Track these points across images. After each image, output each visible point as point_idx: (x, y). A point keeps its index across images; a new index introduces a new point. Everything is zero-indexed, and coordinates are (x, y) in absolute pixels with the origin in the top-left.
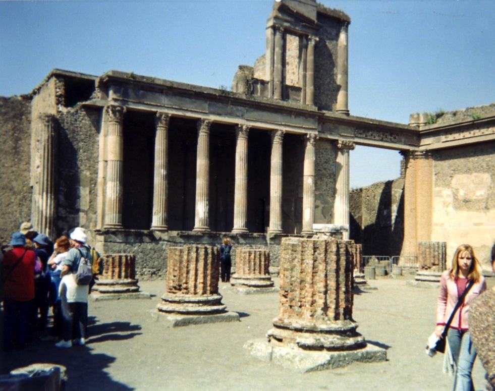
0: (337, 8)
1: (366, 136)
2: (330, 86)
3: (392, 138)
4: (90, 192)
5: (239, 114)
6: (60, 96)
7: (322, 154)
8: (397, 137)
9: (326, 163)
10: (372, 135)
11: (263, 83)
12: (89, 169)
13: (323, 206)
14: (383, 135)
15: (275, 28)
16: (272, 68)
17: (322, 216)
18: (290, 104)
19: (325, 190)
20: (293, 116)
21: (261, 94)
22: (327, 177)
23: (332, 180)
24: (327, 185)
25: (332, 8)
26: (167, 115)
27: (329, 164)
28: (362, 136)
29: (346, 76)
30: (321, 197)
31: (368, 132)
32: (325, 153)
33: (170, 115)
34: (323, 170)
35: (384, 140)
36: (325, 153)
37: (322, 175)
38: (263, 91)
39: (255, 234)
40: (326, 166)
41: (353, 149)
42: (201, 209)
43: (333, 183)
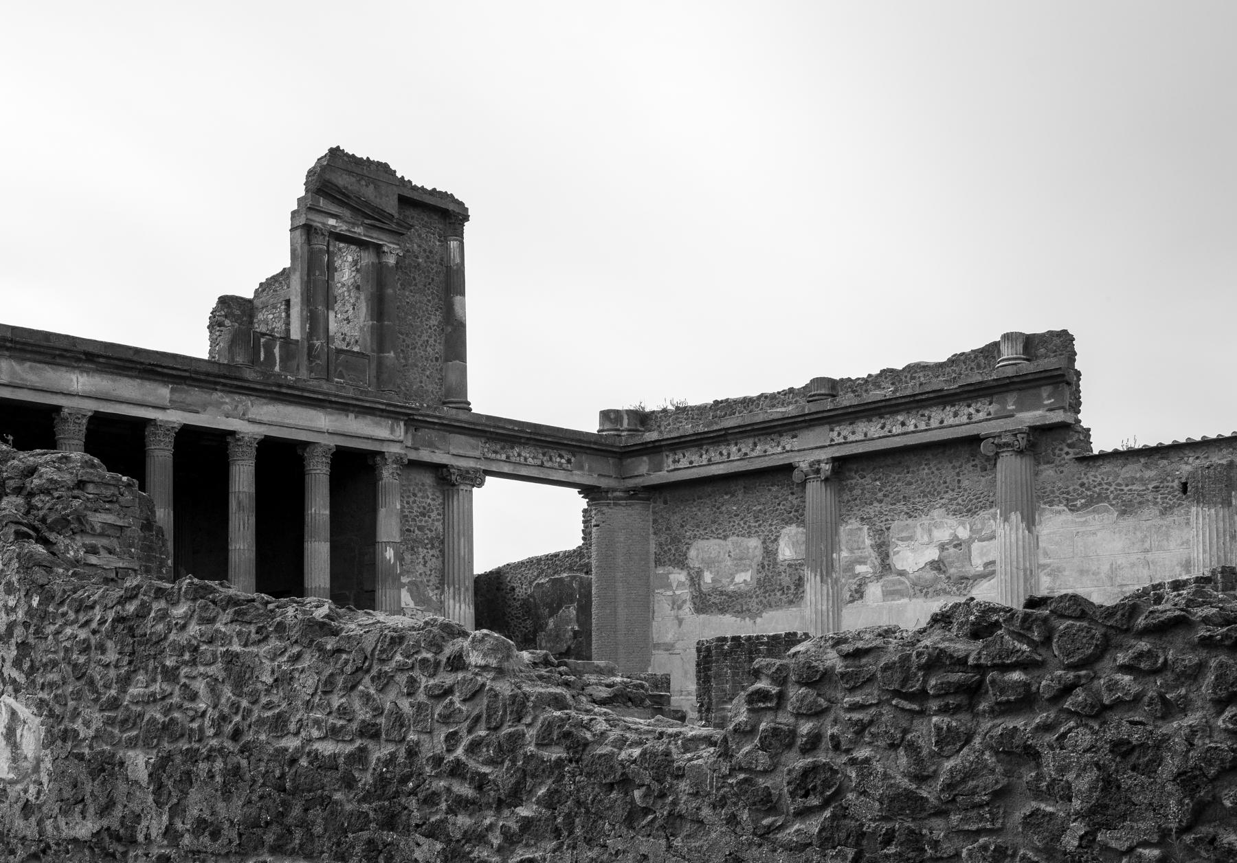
1: (508, 457)
2: (429, 349)
7: (415, 495)
9: (424, 515)
10: (519, 455)
14: (544, 455)
20: (352, 416)
22: (425, 546)
24: (425, 565)
26: (77, 414)
28: (498, 457)
31: (513, 448)
32: (420, 494)
33: (90, 414)
36: (420, 494)
37: (415, 541)
41: (480, 485)
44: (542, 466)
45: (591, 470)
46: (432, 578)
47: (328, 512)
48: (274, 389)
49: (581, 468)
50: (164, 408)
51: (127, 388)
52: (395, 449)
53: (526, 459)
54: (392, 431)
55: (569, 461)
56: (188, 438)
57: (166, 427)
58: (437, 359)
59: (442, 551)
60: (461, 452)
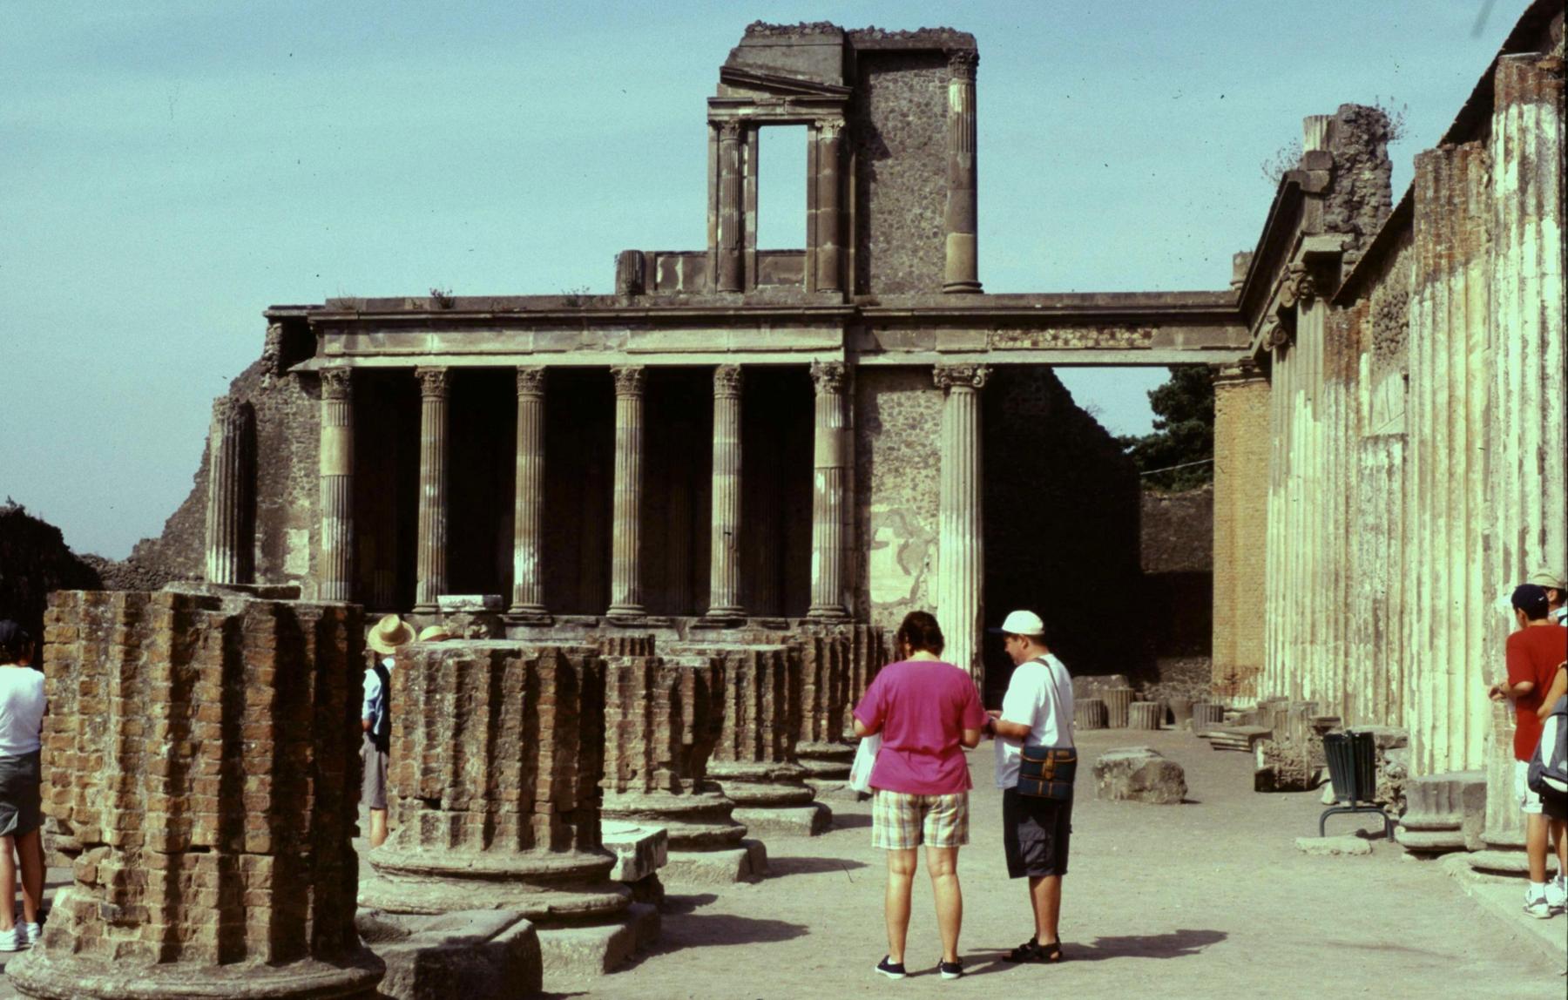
0: (933, 23)
1: (1035, 343)
2: (923, 224)
3: (1135, 336)
4: (311, 538)
5: (613, 342)
6: (270, 358)
7: (900, 404)
8: (1154, 332)
9: (913, 427)
10: (1055, 338)
12: (309, 495)
13: (902, 541)
15: (716, 125)
16: (713, 219)
17: (899, 568)
18: (767, 293)
21: (684, 282)
23: (931, 472)
24: (914, 489)
25: (913, 28)
28: (1018, 344)
29: (963, 195)
30: (897, 519)
34: (903, 447)
38: (689, 278)
39: (650, 620)
40: (913, 436)
42: (523, 565)
43: (933, 478)
44: (1096, 348)
45: (1187, 342)
46: (925, 504)
47: (733, 440)
49: (1169, 342)
56: (554, 378)
58: (935, 234)
59: (938, 470)
60: (955, 347)
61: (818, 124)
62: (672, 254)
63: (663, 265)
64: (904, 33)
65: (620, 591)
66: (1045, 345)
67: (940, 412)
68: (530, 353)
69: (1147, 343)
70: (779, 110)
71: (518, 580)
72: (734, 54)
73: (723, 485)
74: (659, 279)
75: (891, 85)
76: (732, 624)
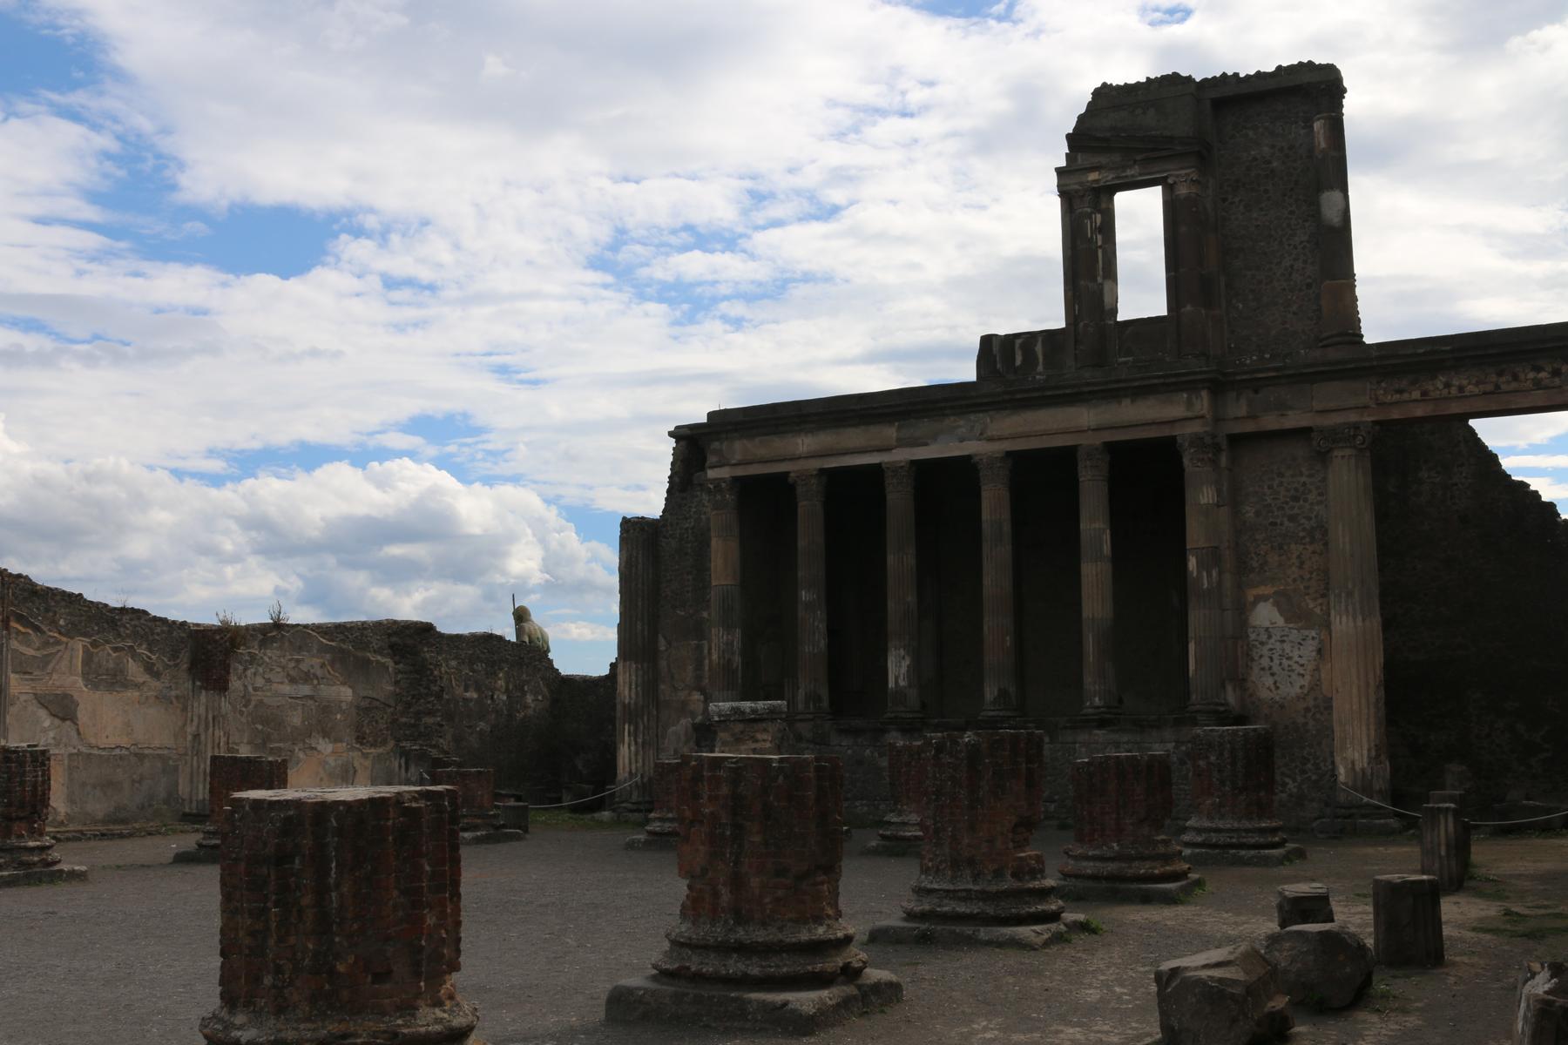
1: (1424, 394)
3: (1543, 375)
7: (1281, 475)
9: (1296, 499)
10: (1447, 385)
11: (1049, 335)
19: (1295, 580)
20: (1126, 402)
24: (1301, 567)
25: (1271, 68)
27: (1306, 500)
28: (1406, 396)
34: (1286, 523)
35: (1504, 387)
42: (898, 668)
48: (1007, 397)
50: (888, 449)
51: (853, 437)
52: (1195, 428)
53: (1461, 389)
54: (1189, 404)
55: (1556, 373)
57: (896, 469)
59: (1326, 544)
61: (1170, 181)
62: (1030, 337)
63: (1022, 346)
64: (1259, 75)
65: (990, 692)
66: (1436, 394)
67: (1324, 480)
68: (897, 452)
69: (1557, 381)
70: (1129, 172)
71: (891, 684)
72: (1081, 118)
73: (1095, 576)
74: (1018, 362)
75: (1251, 133)
76: (1102, 723)
